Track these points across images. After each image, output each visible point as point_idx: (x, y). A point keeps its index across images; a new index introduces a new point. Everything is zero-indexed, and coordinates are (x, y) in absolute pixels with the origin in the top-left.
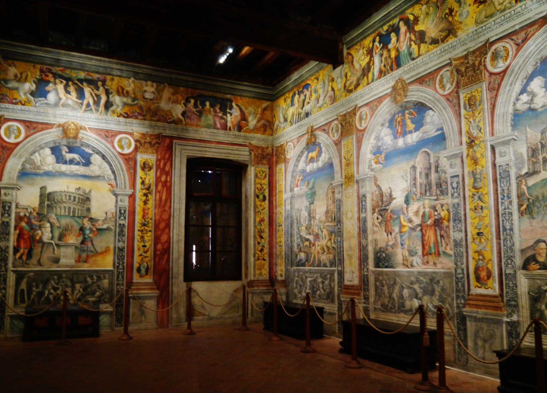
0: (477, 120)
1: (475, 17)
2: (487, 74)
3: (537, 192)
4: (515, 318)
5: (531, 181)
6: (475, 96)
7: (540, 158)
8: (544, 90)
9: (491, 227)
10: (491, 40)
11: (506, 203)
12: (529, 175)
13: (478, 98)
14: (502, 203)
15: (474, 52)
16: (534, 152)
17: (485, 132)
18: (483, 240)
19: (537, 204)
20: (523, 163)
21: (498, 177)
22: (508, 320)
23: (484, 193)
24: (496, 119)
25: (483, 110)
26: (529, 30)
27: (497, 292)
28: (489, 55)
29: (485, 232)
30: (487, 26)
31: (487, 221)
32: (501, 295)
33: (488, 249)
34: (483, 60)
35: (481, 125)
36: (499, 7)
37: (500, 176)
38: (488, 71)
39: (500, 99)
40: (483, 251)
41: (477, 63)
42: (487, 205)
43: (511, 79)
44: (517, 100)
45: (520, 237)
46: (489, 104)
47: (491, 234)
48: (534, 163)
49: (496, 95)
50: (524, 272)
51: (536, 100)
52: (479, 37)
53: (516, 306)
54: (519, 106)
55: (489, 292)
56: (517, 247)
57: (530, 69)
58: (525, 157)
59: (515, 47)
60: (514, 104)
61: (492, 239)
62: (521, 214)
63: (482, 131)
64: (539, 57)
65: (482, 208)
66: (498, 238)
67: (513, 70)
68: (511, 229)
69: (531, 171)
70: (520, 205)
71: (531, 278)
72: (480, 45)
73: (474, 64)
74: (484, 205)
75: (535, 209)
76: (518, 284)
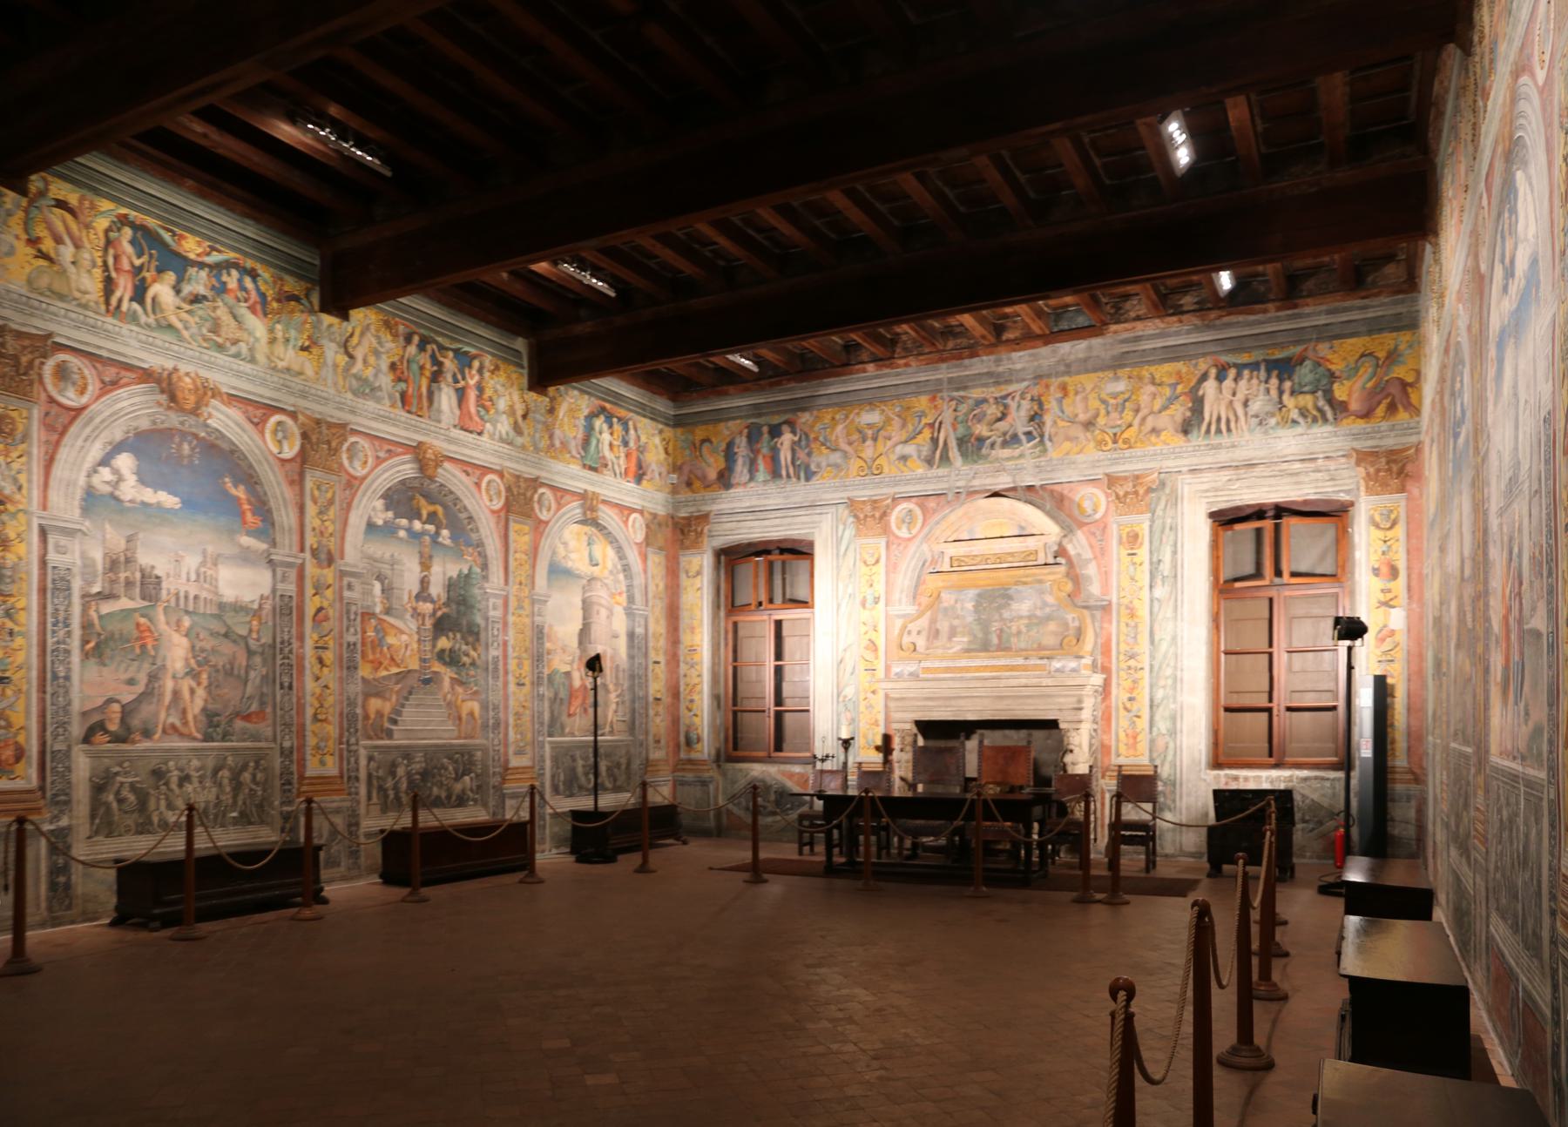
0: (15, 466)
1: (28, 270)
2: (43, 396)
3: (114, 626)
4: (64, 822)
5: (107, 608)
6: (13, 422)
7: (122, 576)
8: (134, 478)
9: (29, 669)
10: (58, 340)
11: (61, 633)
12: (104, 596)
13: (20, 428)
14: (54, 632)
15: (19, 335)
16: (113, 565)
17: (30, 499)
18: (9, 692)
19: (111, 644)
20: (96, 576)
21: (50, 585)
22: (52, 827)
23: (20, 605)
24: (52, 483)
25: (28, 454)
26: (123, 373)
27: (34, 782)
28: (50, 364)
29: (15, 677)
30: (52, 309)
31: (20, 658)
32: (42, 788)
33: (20, 706)
34: (37, 362)
35: (22, 478)
36: (77, 294)
37: (53, 585)
38: (45, 390)
39: (63, 454)
40: (8, 712)
41: (24, 360)
42: (23, 629)
43: (88, 430)
44: (96, 472)
45: (81, 691)
46: (43, 450)
47: (29, 682)
48: (112, 582)
49: (58, 443)
50: (85, 747)
51: (123, 486)
52: (32, 315)
53: (68, 803)
54: (96, 480)
55: (19, 784)
56: (76, 706)
57: (118, 435)
58: (100, 567)
59: (98, 385)
60: (89, 476)
61: (28, 692)
62: (86, 655)
63: (24, 491)
64: (134, 424)
65: (11, 633)
66: (42, 688)
67: (91, 419)
68: (67, 678)
69: (107, 592)
70: (85, 642)
71: (95, 756)
72: (34, 331)
73: (16, 358)
74: (16, 629)
75: (108, 652)
76: (73, 766)
